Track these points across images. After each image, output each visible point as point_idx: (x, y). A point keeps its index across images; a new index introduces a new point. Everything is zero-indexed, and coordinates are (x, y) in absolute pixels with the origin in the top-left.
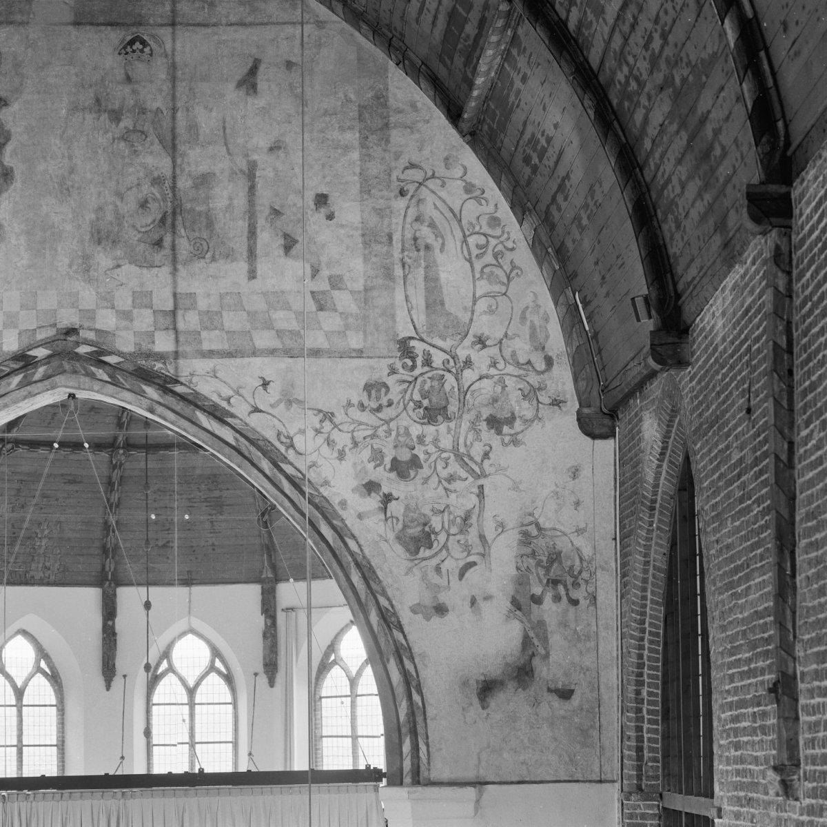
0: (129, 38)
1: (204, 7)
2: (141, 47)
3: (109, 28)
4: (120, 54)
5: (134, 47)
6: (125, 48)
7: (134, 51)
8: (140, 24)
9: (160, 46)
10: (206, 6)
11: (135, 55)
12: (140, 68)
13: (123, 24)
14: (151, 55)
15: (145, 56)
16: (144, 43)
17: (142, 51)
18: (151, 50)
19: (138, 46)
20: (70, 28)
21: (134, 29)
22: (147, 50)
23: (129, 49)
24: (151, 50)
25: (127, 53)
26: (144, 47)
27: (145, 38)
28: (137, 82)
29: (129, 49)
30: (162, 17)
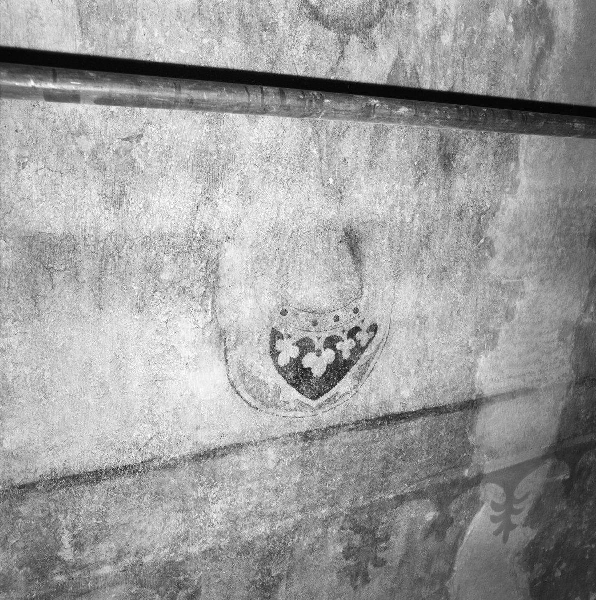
0: (345, 384)
1: (78, 546)
2: (309, 361)
3: (397, 409)
4: (374, 329)
5: (329, 356)
6: (358, 350)
7: (331, 342)
8: (307, 437)
9: (244, 372)
10: (68, 554)
11: (329, 328)
12: (314, 290)
13: (358, 426)
14: (276, 336)
15: (295, 330)
16: (299, 376)
17: (305, 346)
18: (274, 353)
19: (318, 365)
20: (487, 393)
21: (328, 417)
22: (288, 352)
23: (346, 347)
24: (274, 353)
25: (353, 333)
26: (296, 363)
27: (292, 395)
28: (329, 227)
29: (346, 347)
30: (236, 478)
